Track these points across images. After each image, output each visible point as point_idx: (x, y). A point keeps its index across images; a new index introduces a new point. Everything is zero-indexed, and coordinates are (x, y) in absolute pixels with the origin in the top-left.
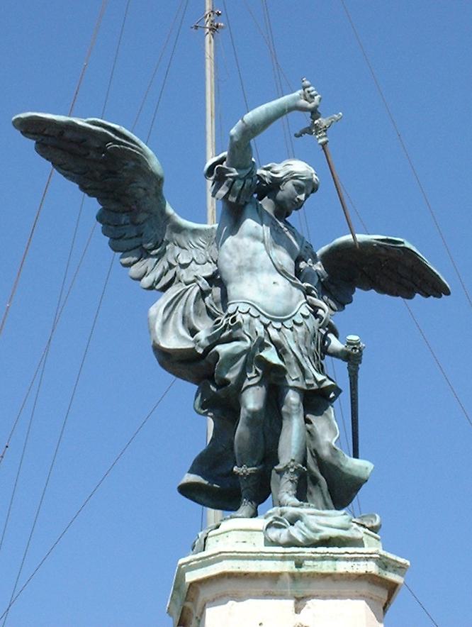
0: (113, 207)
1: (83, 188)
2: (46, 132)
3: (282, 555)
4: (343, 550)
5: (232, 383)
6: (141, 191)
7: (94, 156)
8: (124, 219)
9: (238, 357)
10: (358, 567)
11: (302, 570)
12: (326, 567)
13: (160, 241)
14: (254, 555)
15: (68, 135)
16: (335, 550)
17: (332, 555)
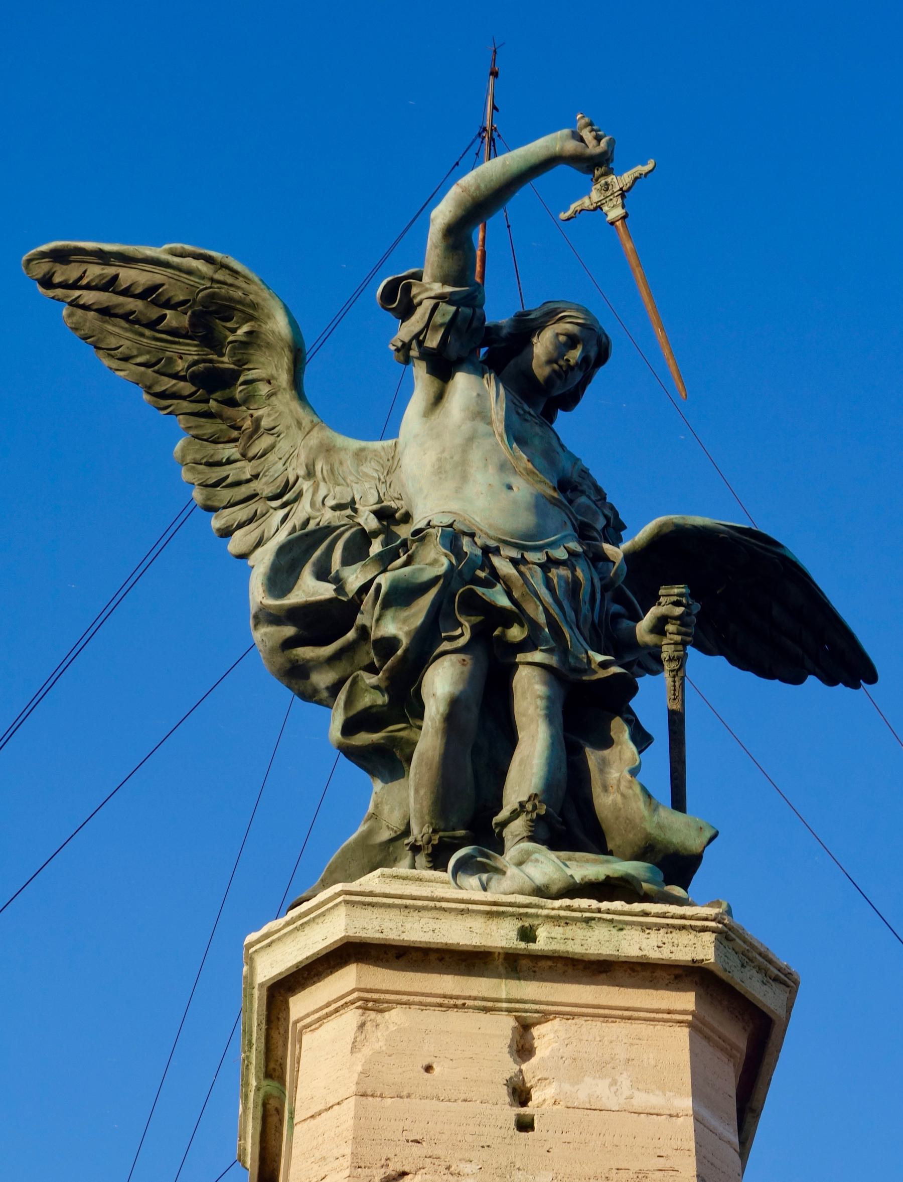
0: (209, 427)
2: (84, 282)
3: (487, 908)
4: (637, 907)
5: (405, 642)
7: (174, 324)
8: (230, 451)
9: (423, 588)
10: (673, 949)
12: (597, 942)
13: (291, 481)
14: (419, 903)
16: (618, 905)
17: (609, 917)
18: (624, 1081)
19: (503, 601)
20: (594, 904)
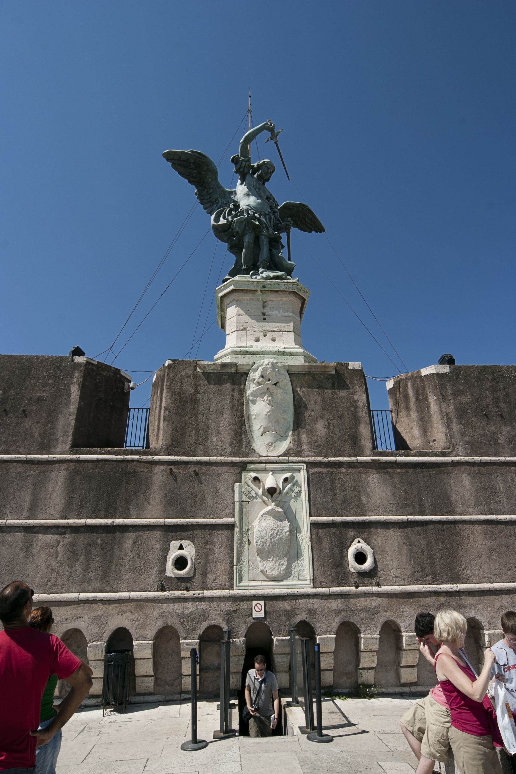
1: (190, 182)
6: (210, 180)
11: (265, 289)
15: (182, 159)
16: (279, 281)
18: (281, 311)
19: (257, 223)
20: (275, 280)
